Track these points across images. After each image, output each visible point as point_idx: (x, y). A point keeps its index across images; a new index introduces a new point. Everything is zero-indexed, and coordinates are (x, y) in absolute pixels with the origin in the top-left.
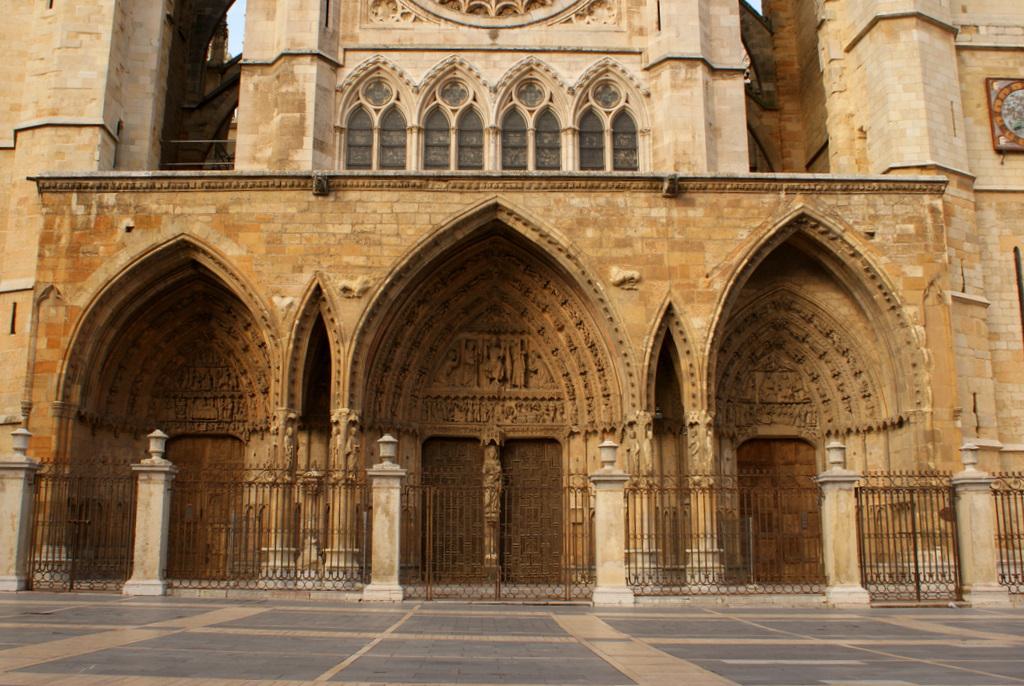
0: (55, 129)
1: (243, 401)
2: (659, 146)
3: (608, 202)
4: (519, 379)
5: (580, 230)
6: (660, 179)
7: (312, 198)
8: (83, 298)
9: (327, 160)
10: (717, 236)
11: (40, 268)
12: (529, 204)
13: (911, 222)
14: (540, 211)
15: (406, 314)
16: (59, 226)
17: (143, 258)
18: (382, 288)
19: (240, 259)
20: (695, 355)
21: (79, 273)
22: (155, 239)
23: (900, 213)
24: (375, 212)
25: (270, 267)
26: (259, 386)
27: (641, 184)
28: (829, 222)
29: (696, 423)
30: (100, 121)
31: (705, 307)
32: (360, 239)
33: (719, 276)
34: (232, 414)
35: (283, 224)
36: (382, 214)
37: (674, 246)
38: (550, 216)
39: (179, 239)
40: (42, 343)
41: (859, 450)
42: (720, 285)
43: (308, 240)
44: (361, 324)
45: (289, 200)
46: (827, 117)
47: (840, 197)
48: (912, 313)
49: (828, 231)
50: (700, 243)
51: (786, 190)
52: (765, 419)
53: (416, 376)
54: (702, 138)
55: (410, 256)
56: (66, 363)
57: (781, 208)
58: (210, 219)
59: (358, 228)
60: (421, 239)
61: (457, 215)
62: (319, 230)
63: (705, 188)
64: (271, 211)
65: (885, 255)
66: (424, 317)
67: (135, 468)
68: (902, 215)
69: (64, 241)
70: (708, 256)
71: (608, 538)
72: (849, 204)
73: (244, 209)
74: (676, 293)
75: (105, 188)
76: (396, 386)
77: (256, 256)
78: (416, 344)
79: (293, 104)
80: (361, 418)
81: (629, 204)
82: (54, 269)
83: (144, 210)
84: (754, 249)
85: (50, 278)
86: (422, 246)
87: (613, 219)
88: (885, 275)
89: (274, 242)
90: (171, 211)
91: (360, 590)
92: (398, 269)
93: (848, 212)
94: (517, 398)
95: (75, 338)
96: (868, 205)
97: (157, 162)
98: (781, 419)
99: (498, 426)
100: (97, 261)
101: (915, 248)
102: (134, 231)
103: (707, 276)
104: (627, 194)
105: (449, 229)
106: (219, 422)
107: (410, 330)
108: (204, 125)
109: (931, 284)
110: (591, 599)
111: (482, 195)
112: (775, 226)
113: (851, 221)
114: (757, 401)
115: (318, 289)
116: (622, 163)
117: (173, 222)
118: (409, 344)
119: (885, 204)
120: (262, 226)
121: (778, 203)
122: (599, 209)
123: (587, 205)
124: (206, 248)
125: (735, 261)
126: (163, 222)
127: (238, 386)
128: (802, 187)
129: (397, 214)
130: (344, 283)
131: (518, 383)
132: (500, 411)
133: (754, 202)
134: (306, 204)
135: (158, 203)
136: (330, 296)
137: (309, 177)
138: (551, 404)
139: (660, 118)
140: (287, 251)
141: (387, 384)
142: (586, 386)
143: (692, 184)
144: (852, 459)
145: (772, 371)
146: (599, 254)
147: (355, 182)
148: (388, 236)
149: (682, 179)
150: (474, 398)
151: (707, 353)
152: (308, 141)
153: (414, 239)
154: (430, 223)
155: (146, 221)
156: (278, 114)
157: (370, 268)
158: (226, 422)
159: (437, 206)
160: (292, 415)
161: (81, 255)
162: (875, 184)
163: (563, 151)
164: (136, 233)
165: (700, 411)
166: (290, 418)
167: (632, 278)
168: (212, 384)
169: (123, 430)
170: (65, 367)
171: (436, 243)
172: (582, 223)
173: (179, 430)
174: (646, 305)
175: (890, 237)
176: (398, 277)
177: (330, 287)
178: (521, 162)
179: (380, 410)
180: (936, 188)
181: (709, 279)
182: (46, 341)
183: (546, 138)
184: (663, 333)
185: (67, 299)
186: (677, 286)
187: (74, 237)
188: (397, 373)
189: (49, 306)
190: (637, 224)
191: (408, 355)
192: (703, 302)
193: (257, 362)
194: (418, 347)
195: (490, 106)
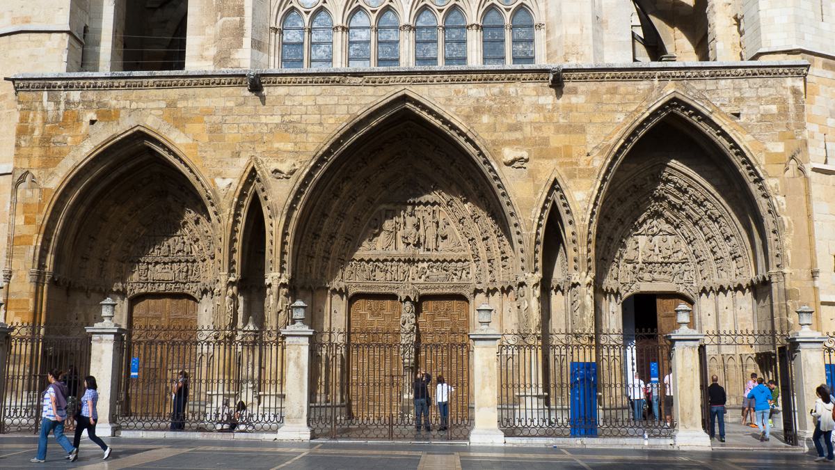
0: (28, 34)
1: (196, 264)
2: (551, 38)
3: (501, 92)
4: (432, 245)
5: (476, 116)
6: (546, 71)
7: (248, 93)
8: (55, 182)
9: (263, 57)
10: (597, 119)
11: (17, 156)
12: (433, 95)
13: (774, 103)
14: (443, 101)
15: (332, 189)
16: (33, 120)
17: (105, 147)
18: (307, 170)
19: (187, 146)
20: (577, 224)
21: (50, 161)
22: (114, 130)
23: (763, 95)
24: (301, 104)
25: (214, 153)
26: (209, 252)
27: (530, 75)
28: (697, 105)
29: (578, 284)
30: (69, 29)
31: (585, 182)
32: (288, 127)
33: (598, 155)
34: (187, 276)
35: (223, 116)
36: (307, 106)
37: (559, 129)
38: (450, 105)
39: (135, 130)
40: (20, 220)
41: (731, 307)
42: (599, 163)
43: (245, 129)
44: (290, 201)
45: (228, 95)
46: (707, 6)
47: (708, 82)
48: (773, 186)
49: (697, 112)
50: (582, 125)
51: (659, 77)
52: (647, 276)
53: (342, 242)
54: (589, 31)
55: (331, 142)
56: (41, 236)
57: (654, 94)
58: (160, 112)
59: (286, 118)
60: (340, 127)
61: (371, 105)
62: (254, 121)
63: (586, 78)
64: (213, 105)
65: (748, 133)
66: (349, 191)
67: (89, 330)
68: (765, 97)
69: (37, 133)
70: (589, 137)
71: (483, 388)
72: (717, 88)
73: (190, 104)
74: (561, 171)
75: (71, 87)
76: (324, 251)
77: (200, 144)
78: (342, 215)
79: (234, 9)
80: (291, 280)
81: (520, 93)
82: (29, 157)
83: (105, 105)
84: (631, 129)
85: (25, 165)
86: (342, 132)
87: (504, 107)
88: (749, 151)
89: (215, 131)
90: (128, 106)
91: (275, 431)
92: (321, 153)
93: (715, 96)
94: (430, 260)
95: (48, 216)
96: (734, 88)
97: (120, 62)
98: (662, 276)
99: (412, 284)
100: (66, 149)
101: (778, 126)
102: (96, 123)
103: (588, 155)
104: (518, 84)
105: (364, 118)
106: (177, 282)
107: (336, 202)
108: (165, 22)
109: (792, 158)
110: (468, 439)
111: (392, 88)
112: (648, 109)
113: (718, 104)
114: (640, 260)
115: (253, 170)
116: (520, 53)
117: (130, 116)
118: (335, 214)
119: (749, 87)
120: (206, 118)
121: (652, 89)
122: (494, 98)
123: (483, 95)
124: (158, 137)
125: (612, 142)
126: (121, 115)
127: (191, 253)
128: (674, 74)
129: (320, 106)
130: (275, 166)
131: (430, 247)
132: (415, 272)
133: (630, 89)
134: (242, 99)
135: (115, 99)
136: (263, 176)
137: (244, 76)
138: (460, 264)
139: (553, 14)
140: (226, 139)
141: (317, 251)
142: (488, 249)
143: (575, 75)
144: (724, 313)
145: (653, 235)
146: (494, 138)
147: (284, 79)
148: (312, 124)
149: (565, 70)
150: (392, 260)
151: (587, 222)
152: (247, 41)
153: (335, 127)
154: (348, 113)
155: (107, 115)
156: (221, 17)
157: (296, 152)
158: (182, 283)
159: (354, 98)
160: (232, 279)
161: (52, 145)
162: (739, 70)
163: (469, 43)
164: (99, 125)
165: (581, 273)
166: (231, 281)
167: (522, 158)
168: (170, 250)
169: (93, 290)
170: (40, 240)
171: (354, 129)
172: (478, 110)
173: (143, 291)
174: (534, 181)
175: (754, 117)
176: (321, 160)
177: (264, 169)
178: (432, 54)
179: (311, 271)
180: (800, 71)
181: (589, 158)
182: (23, 218)
183: (454, 33)
184: (549, 205)
185: (41, 182)
186: (561, 164)
187: (46, 129)
188: (325, 240)
189: (25, 188)
190: (526, 110)
191: (335, 224)
192: (584, 177)
193: (207, 232)
194: (343, 217)
195: (404, 6)
